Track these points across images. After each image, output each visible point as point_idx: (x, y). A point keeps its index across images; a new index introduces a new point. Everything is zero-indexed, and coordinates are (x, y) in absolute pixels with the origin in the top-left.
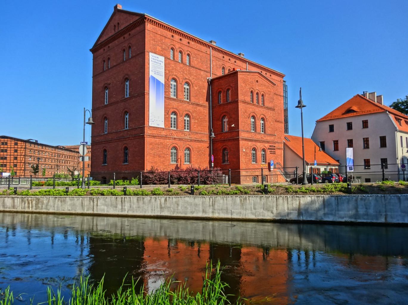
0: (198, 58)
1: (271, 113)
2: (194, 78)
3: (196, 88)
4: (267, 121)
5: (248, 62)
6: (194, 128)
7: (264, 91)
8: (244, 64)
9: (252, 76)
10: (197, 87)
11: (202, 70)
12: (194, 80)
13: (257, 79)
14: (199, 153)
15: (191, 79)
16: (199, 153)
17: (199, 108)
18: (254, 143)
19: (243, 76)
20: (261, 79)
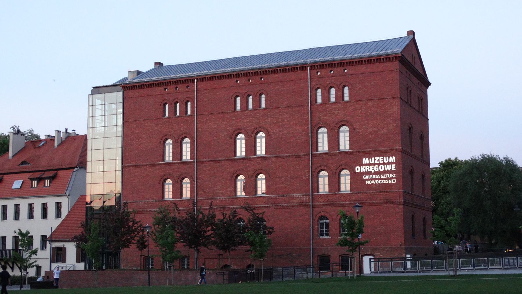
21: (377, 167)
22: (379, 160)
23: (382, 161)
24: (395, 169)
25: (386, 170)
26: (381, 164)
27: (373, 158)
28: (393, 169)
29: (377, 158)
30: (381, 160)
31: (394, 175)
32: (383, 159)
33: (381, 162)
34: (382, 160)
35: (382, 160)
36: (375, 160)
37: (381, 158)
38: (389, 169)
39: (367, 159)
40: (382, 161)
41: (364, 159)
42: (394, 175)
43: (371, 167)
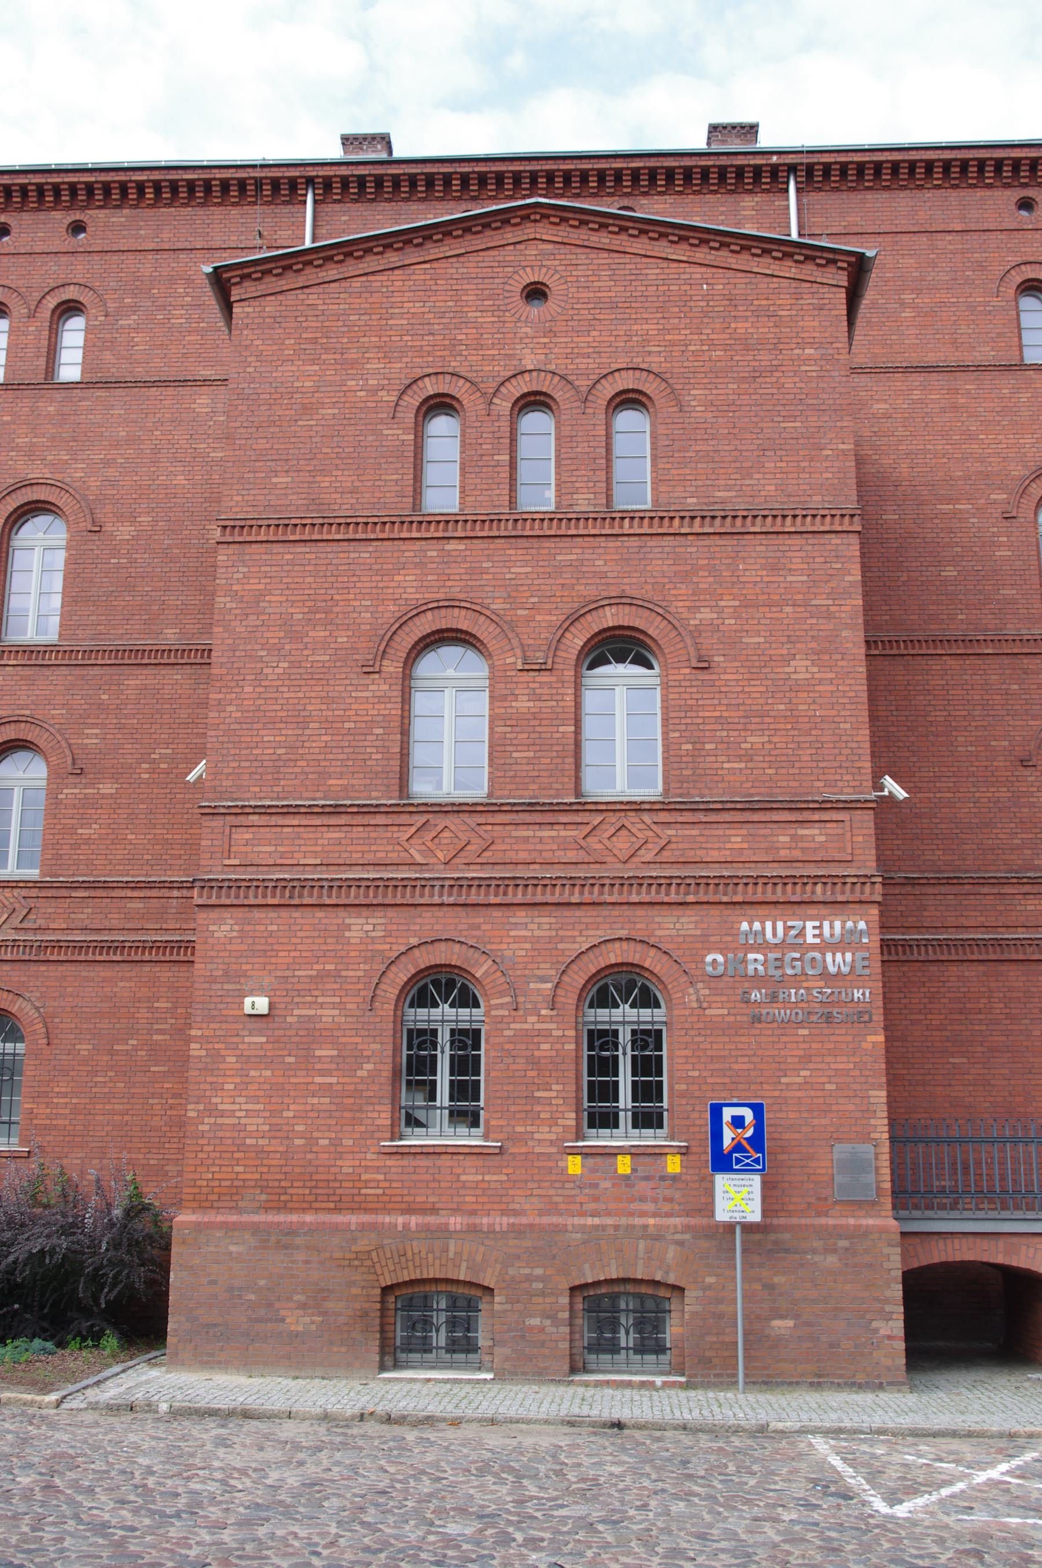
0: (163, 307)
1: (774, 568)
2: (107, 463)
3: (125, 531)
4: (704, 666)
5: (792, 168)
6: (75, 846)
7: (655, 363)
8: (749, 202)
9: (453, 268)
10: (133, 519)
11: (206, 382)
12: (111, 472)
13: (530, 276)
14: (112, 1053)
15: (77, 472)
16: (112, 1053)
17: (135, 681)
18: (429, 923)
19: (312, 297)
20: (603, 258)
21: (794, 959)
22: (802, 933)
23: (815, 936)
24: (867, 971)
25: (832, 970)
26: (813, 947)
27: (780, 925)
28: (859, 971)
29: (799, 924)
30: (810, 932)
31: (863, 994)
32: (820, 927)
33: (810, 940)
34: (817, 932)
35: (817, 932)
36: (787, 929)
37: (809, 924)
38: (845, 970)
39: (757, 926)
40: (815, 936)
41: (745, 926)
42: (863, 994)
43: (772, 956)
